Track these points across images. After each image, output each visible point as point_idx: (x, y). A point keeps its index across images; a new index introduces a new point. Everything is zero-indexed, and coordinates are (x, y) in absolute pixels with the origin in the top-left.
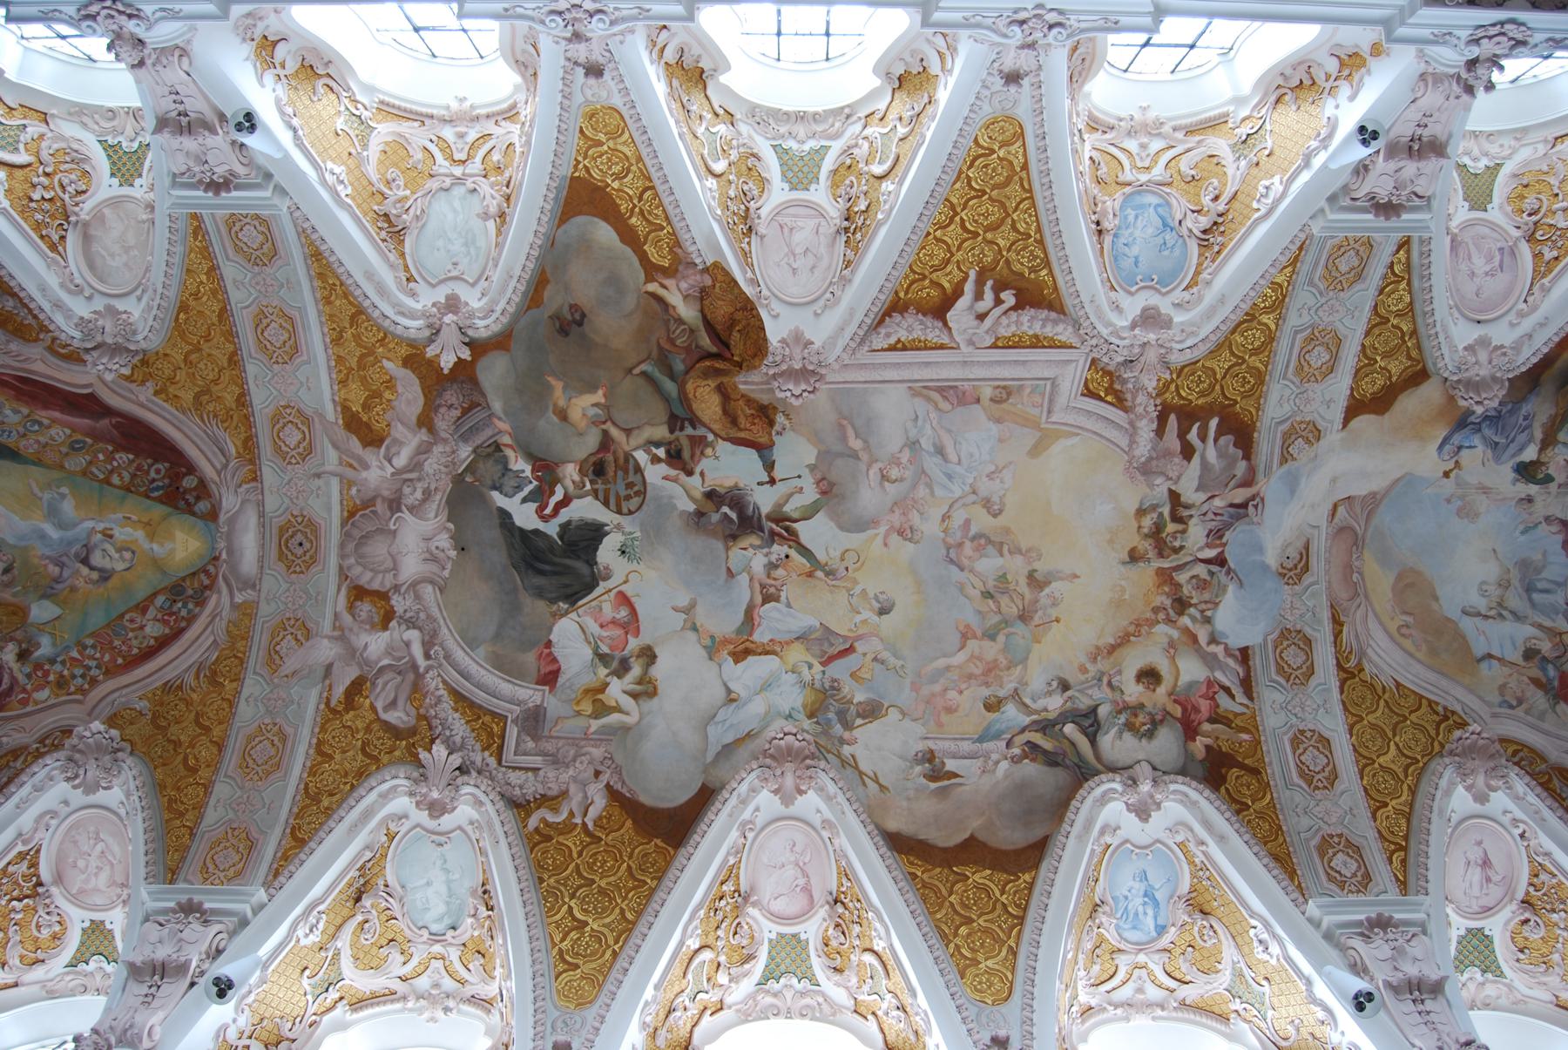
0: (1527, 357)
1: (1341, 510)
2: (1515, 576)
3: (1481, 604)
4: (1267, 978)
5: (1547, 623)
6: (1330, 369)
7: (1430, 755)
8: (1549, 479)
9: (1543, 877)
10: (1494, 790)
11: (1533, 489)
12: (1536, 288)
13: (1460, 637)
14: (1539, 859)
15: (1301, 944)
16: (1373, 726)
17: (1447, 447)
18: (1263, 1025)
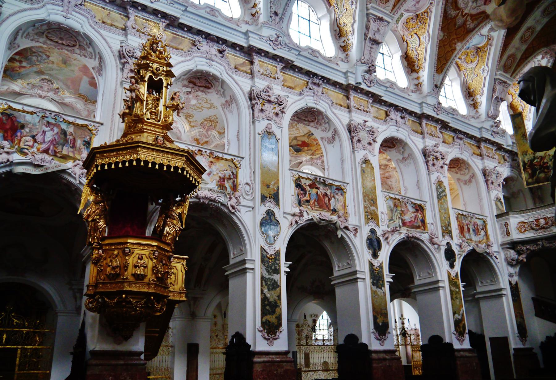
9: (426, 14)
14: (429, 11)
15: (360, 11)
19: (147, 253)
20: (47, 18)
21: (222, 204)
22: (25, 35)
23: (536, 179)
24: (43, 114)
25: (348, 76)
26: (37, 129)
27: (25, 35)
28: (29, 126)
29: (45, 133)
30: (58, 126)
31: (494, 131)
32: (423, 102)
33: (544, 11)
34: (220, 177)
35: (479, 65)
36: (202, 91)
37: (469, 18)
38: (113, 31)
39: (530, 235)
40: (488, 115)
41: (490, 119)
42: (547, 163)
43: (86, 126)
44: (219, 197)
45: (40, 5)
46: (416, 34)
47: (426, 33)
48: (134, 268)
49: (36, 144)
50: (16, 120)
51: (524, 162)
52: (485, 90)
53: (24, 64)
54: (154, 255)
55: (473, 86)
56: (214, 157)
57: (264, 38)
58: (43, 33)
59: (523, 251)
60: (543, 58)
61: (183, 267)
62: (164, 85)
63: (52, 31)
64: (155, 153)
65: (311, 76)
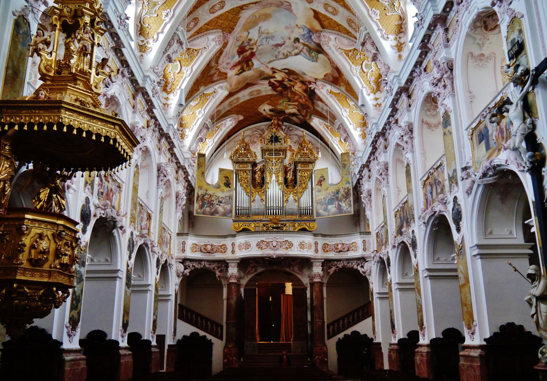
0: (325, 48)
1: (288, 4)
2: (270, 35)
3: (262, 30)
4: (158, 15)
5: (258, 42)
6: (327, 10)
7: (222, 28)
8: (295, 43)
9: (196, 53)
10: (216, 42)
11: (292, 40)
12: (342, 51)
13: (253, 27)
14: (200, 52)
15: (171, 27)
16: (228, 16)
17: (304, 27)
18: (144, 13)
23: (203, 210)
25: (146, 80)
31: (192, 163)
32: (172, 125)
33: (251, 92)
35: (197, 106)
37: (218, 72)
39: (198, 255)
40: (190, 148)
41: (190, 152)
42: (213, 201)
46: (180, 61)
47: (190, 67)
51: (198, 195)
52: (196, 128)
55: (186, 119)
57: (118, 13)
59: (189, 266)
60: (230, 121)
65: (125, 66)
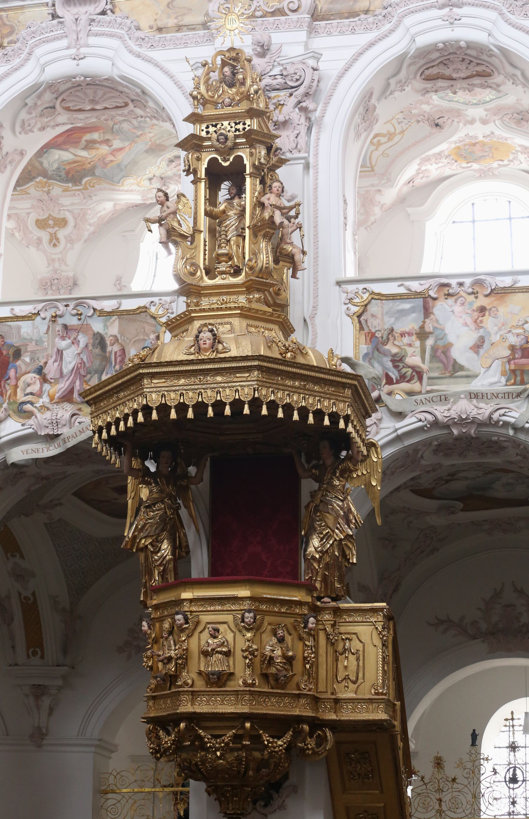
19: (229, 618)
20: (42, 79)
21: (515, 429)
22: (18, 129)
24: (52, 312)
26: (46, 349)
27: (18, 129)
28: (29, 348)
29: (62, 352)
30: (83, 328)
34: (512, 348)
36: (482, 86)
38: (183, 41)
43: (143, 310)
44: (502, 412)
45: (23, 56)
48: (202, 658)
49: (46, 386)
50: (5, 343)
53: (117, 144)
54: (243, 621)
56: (489, 290)
58: (54, 107)
61: (375, 633)
62: (248, 172)
63: (67, 96)
64: (182, 381)
